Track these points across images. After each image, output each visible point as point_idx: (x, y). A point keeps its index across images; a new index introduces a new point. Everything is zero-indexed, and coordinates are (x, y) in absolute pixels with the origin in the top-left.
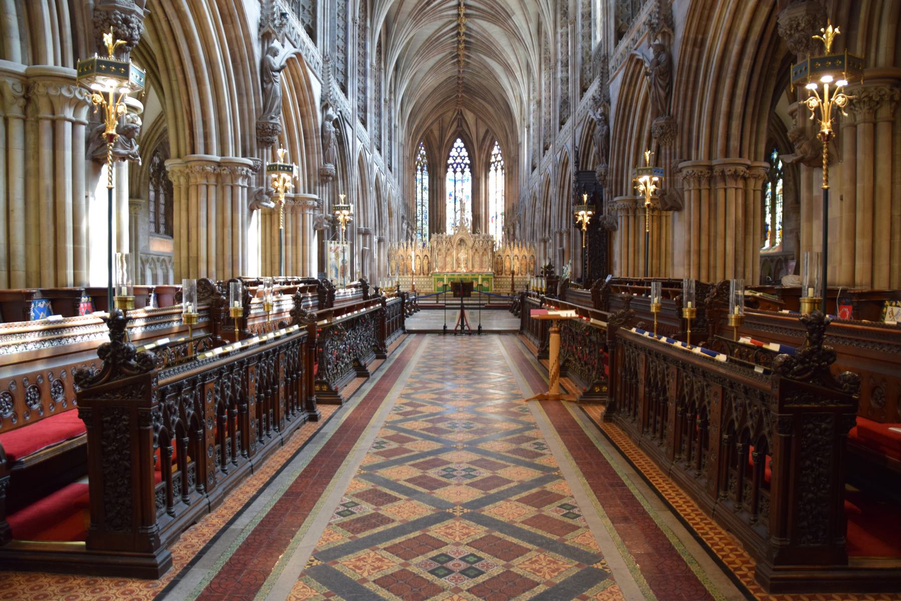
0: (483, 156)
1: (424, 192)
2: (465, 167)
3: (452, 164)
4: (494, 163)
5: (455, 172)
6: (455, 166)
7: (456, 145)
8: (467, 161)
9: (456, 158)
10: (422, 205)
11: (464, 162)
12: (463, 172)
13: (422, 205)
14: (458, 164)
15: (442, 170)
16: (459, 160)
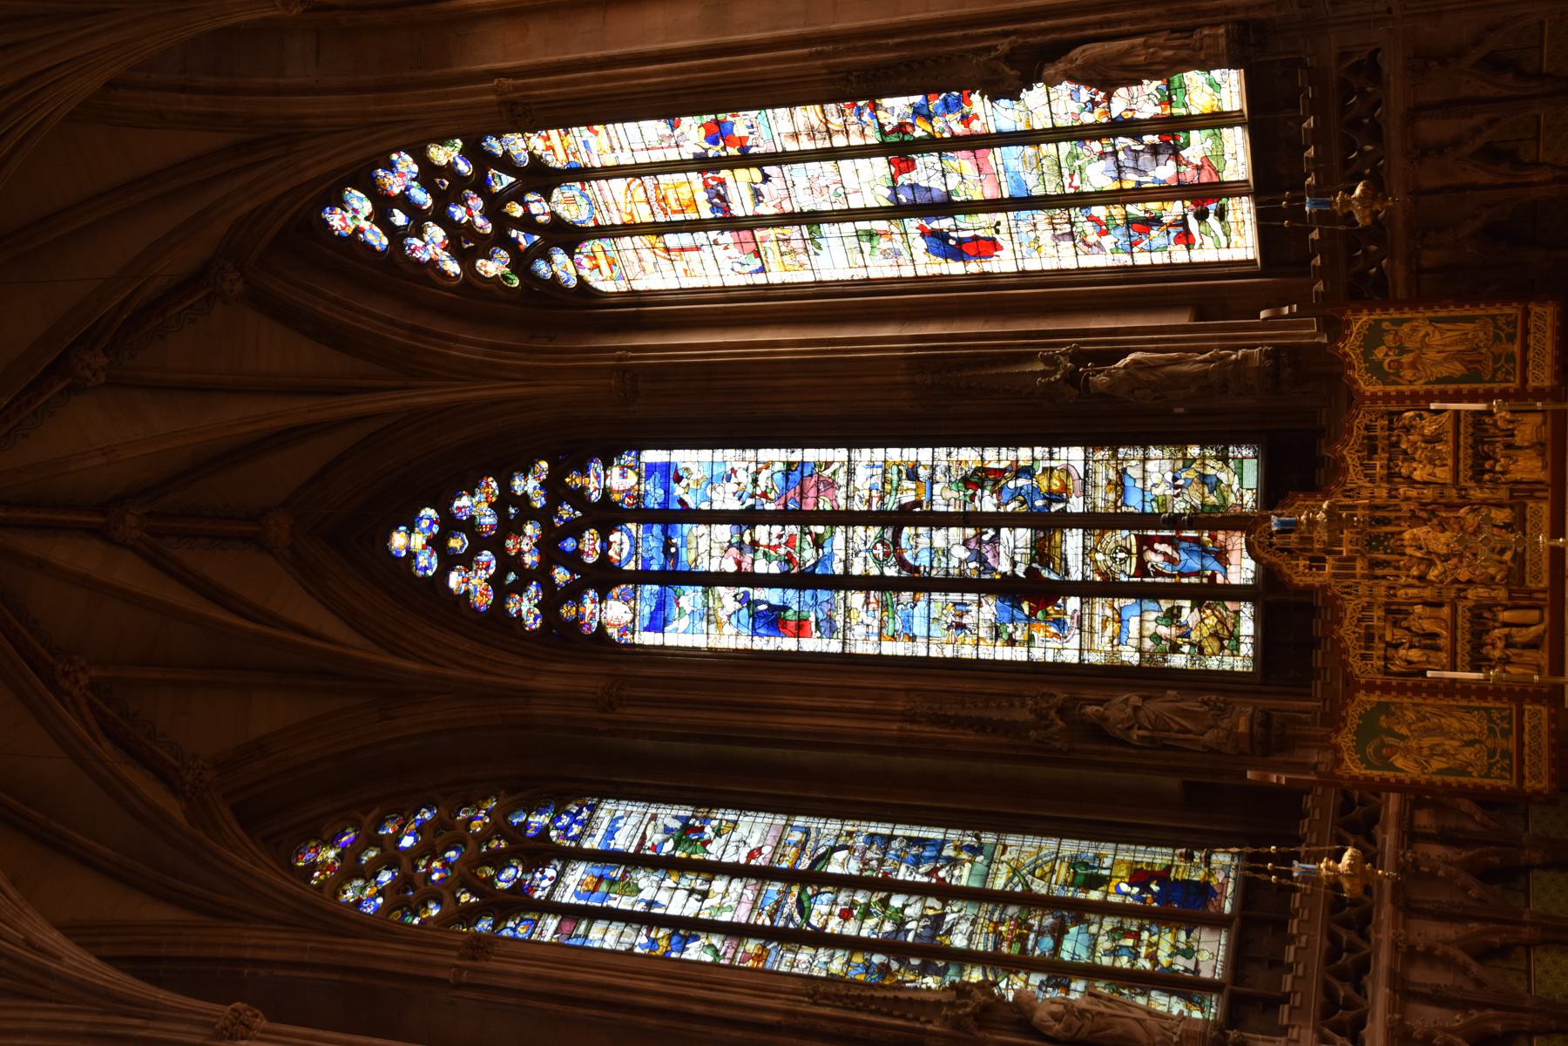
0: (468, 343)
1: (714, 852)
2: (578, 497)
3: (551, 601)
4: (521, 262)
5: (606, 578)
6: (561, 575)
7: (427, 562)
8: (528, 485)
9: (508, 562)
10: (815, 878)
11: (539, 502)
12: (608, 515)
13: (815, 878)
14: (549, 548)
15: (555, 679)
16: (527, 543)
